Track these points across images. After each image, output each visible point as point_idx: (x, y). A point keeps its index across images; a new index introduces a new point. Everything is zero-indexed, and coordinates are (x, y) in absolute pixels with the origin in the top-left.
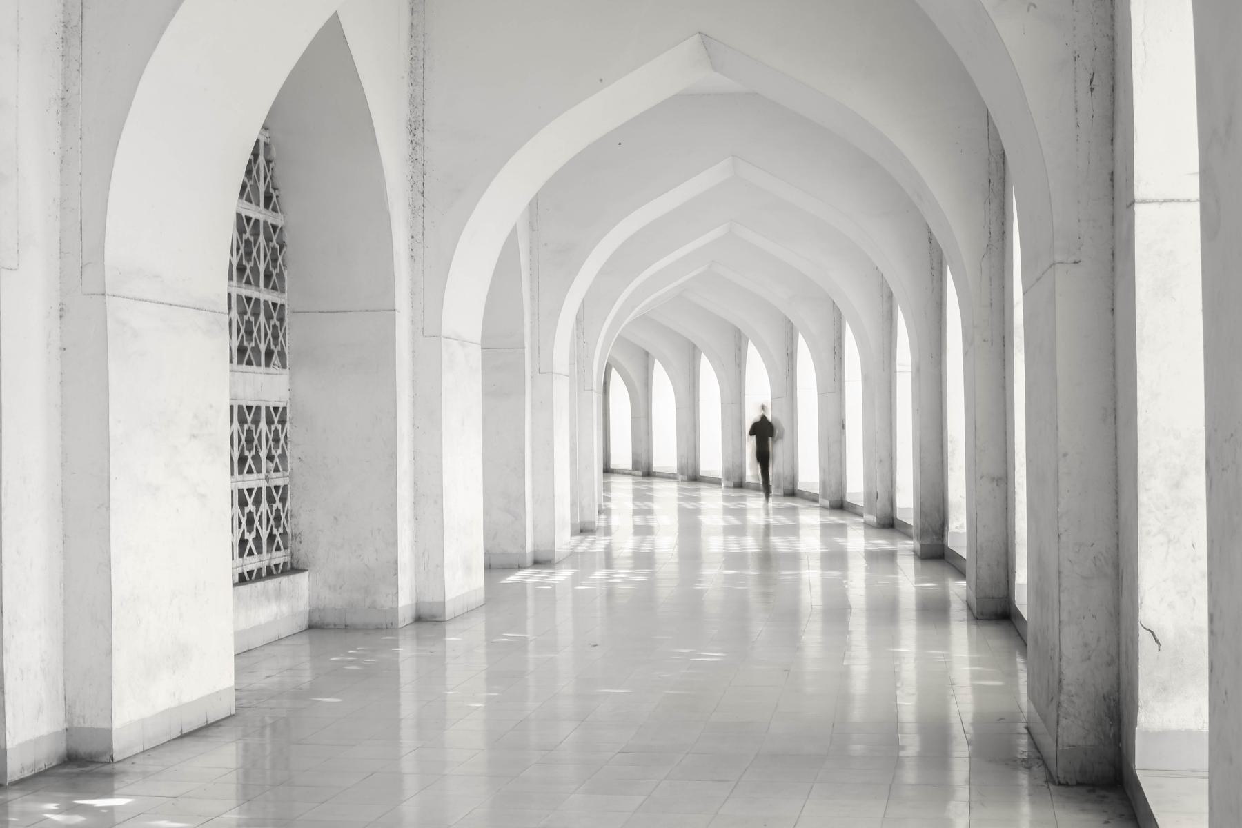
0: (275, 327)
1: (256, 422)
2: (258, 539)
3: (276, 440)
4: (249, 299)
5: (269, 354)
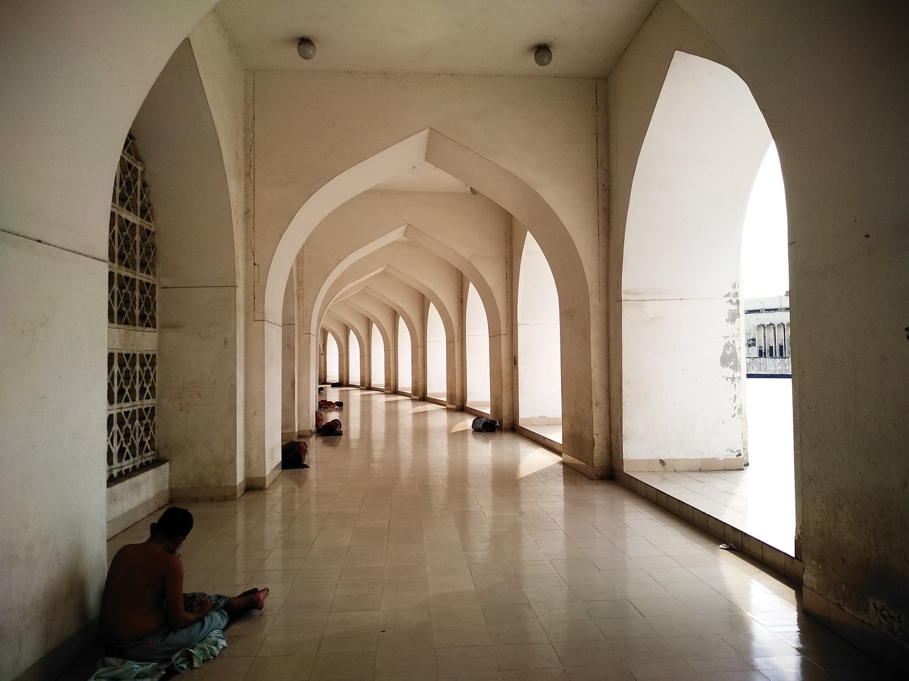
0: (147, 299)
1: (133, 364)
2: (132, 447)
3: (148, 377)
4: (127, 278)
5: (142, 317)
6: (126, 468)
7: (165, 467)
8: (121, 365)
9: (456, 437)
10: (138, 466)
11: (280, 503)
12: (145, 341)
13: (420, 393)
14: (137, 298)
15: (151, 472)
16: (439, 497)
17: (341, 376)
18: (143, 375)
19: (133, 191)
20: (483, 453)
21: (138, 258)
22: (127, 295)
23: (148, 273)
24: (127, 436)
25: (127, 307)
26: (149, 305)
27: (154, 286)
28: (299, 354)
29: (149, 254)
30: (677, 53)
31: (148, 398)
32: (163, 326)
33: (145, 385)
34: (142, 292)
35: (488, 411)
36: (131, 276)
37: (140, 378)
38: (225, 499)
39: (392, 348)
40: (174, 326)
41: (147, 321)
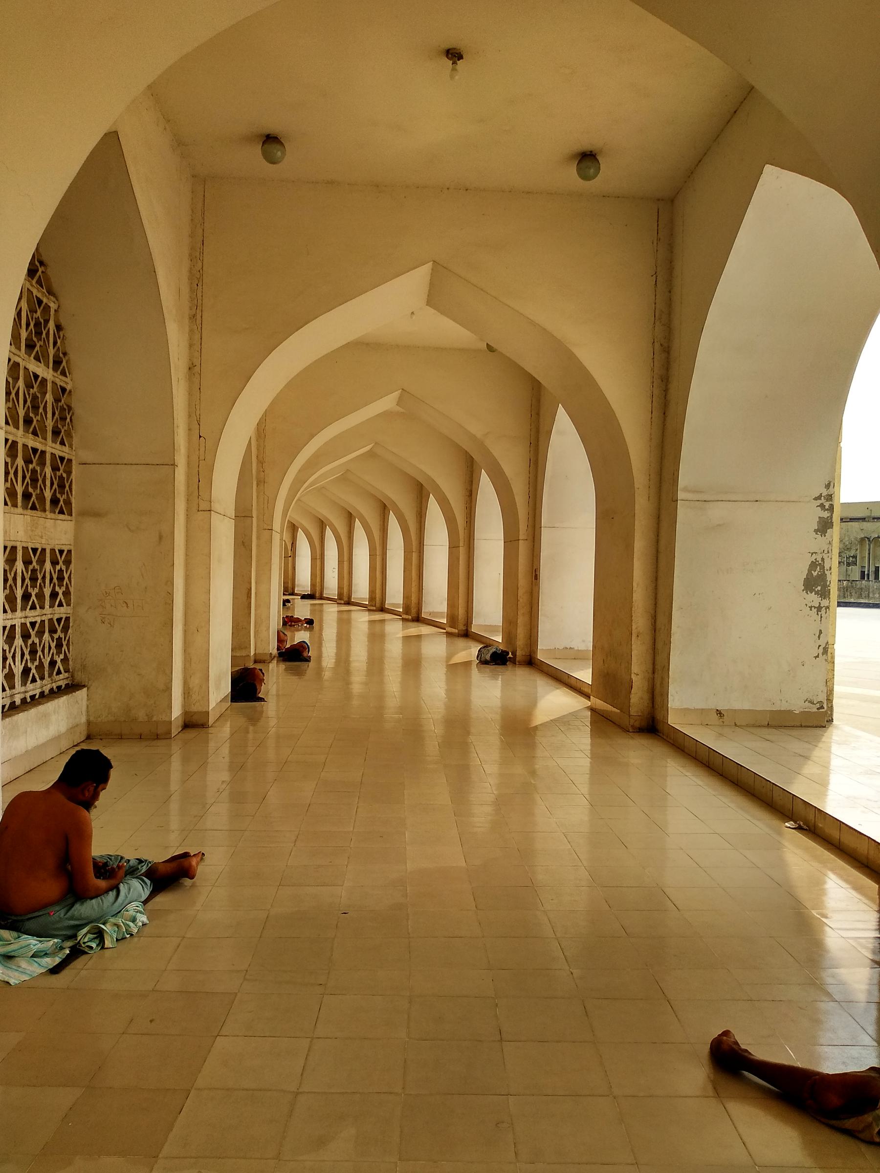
0: (61, 477)
1: (42, 562)
2: (40, 667)
3: (61, 579)
4: (35, 450)
5: (55, 501)
6: (31, 693)
7: (82, 694)
8: (27, 562)
9: (456, 669)
10: (47, 692)
11: (227, 745)
12: (56, 532)
13: (414, 611)
14: (48, 476)
15: (63, 700)
16: (432, 747)
17: (313, 585)
18: (55, 577)
19: (44, 335)
20: (490, 692)
21: (50, 424)
22: (34, 471)
23: (62, 443)
24: (33, 652)
25: (35, 488)
26: (62, 485)
27: (70, 461)
28: (257, 556)
29: (63, 419)
30: (768, 168)
31: (61, 605)
32: (83, 514)
33: (57, 589)
34: (55, 469)
35: (499, 639)
36: (40, 447)
37: (51, 579)
38: (157, 737)
39: (378, 552)
40: (96, 514)
41: (60, 505)
